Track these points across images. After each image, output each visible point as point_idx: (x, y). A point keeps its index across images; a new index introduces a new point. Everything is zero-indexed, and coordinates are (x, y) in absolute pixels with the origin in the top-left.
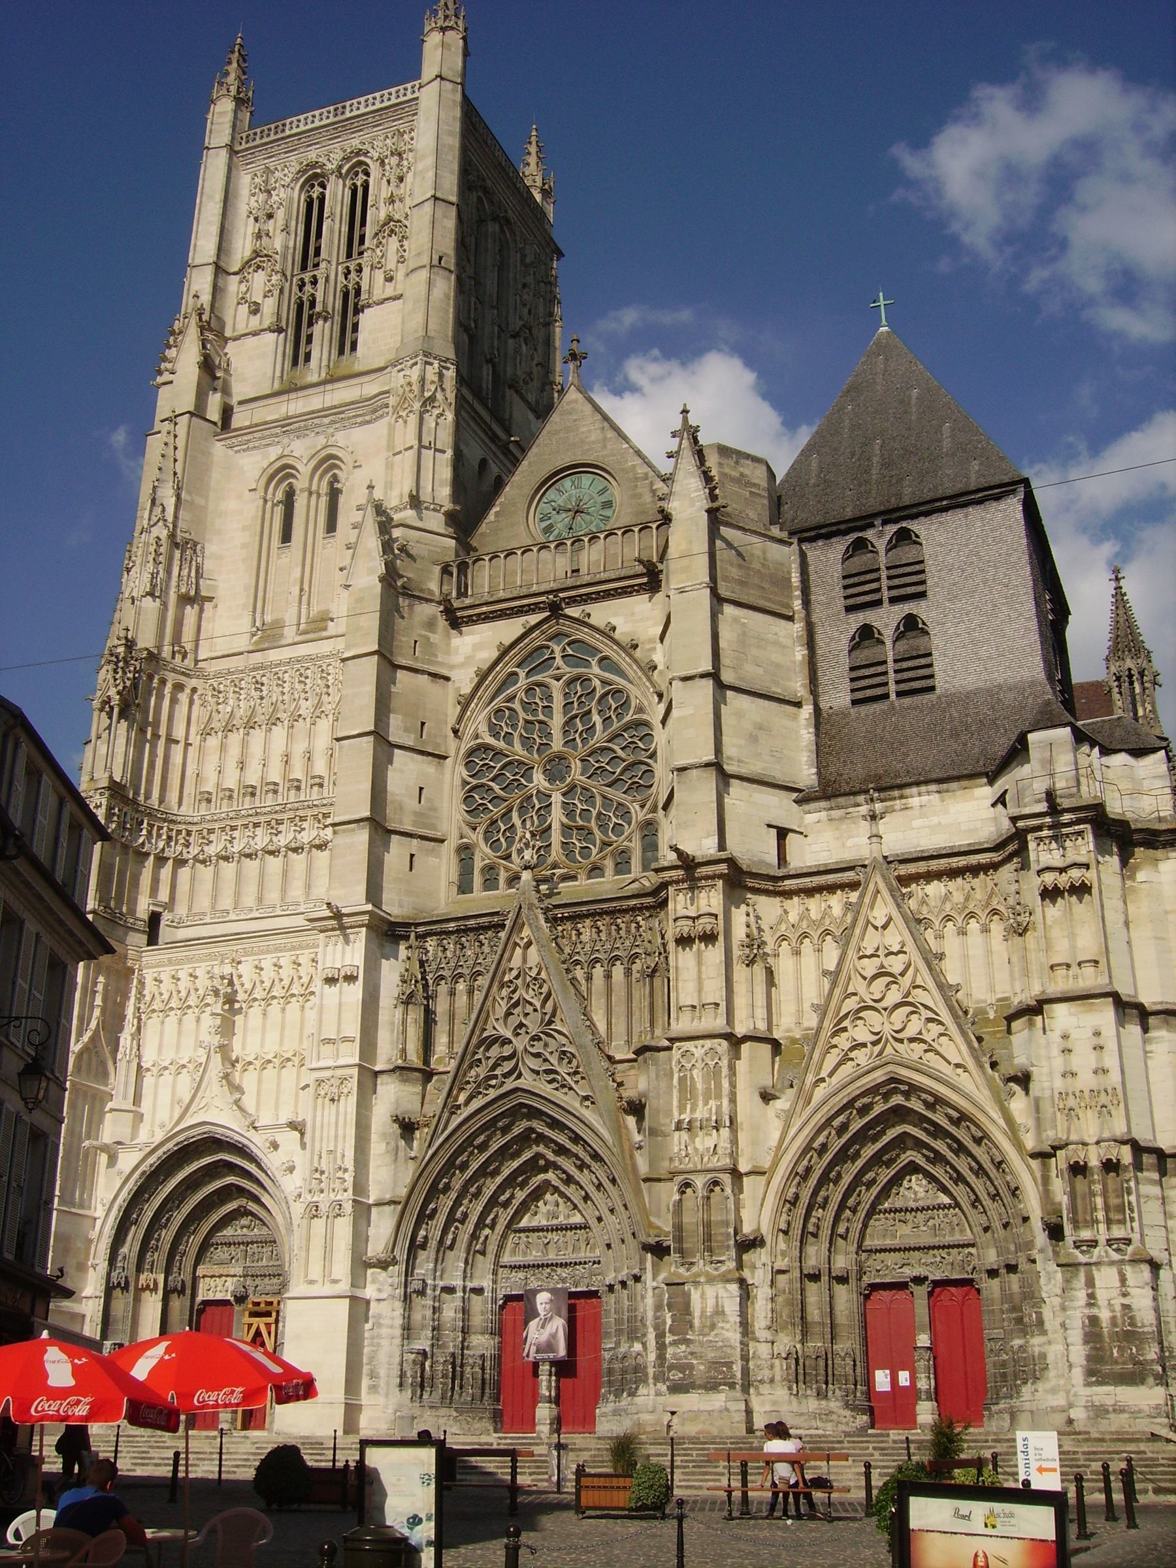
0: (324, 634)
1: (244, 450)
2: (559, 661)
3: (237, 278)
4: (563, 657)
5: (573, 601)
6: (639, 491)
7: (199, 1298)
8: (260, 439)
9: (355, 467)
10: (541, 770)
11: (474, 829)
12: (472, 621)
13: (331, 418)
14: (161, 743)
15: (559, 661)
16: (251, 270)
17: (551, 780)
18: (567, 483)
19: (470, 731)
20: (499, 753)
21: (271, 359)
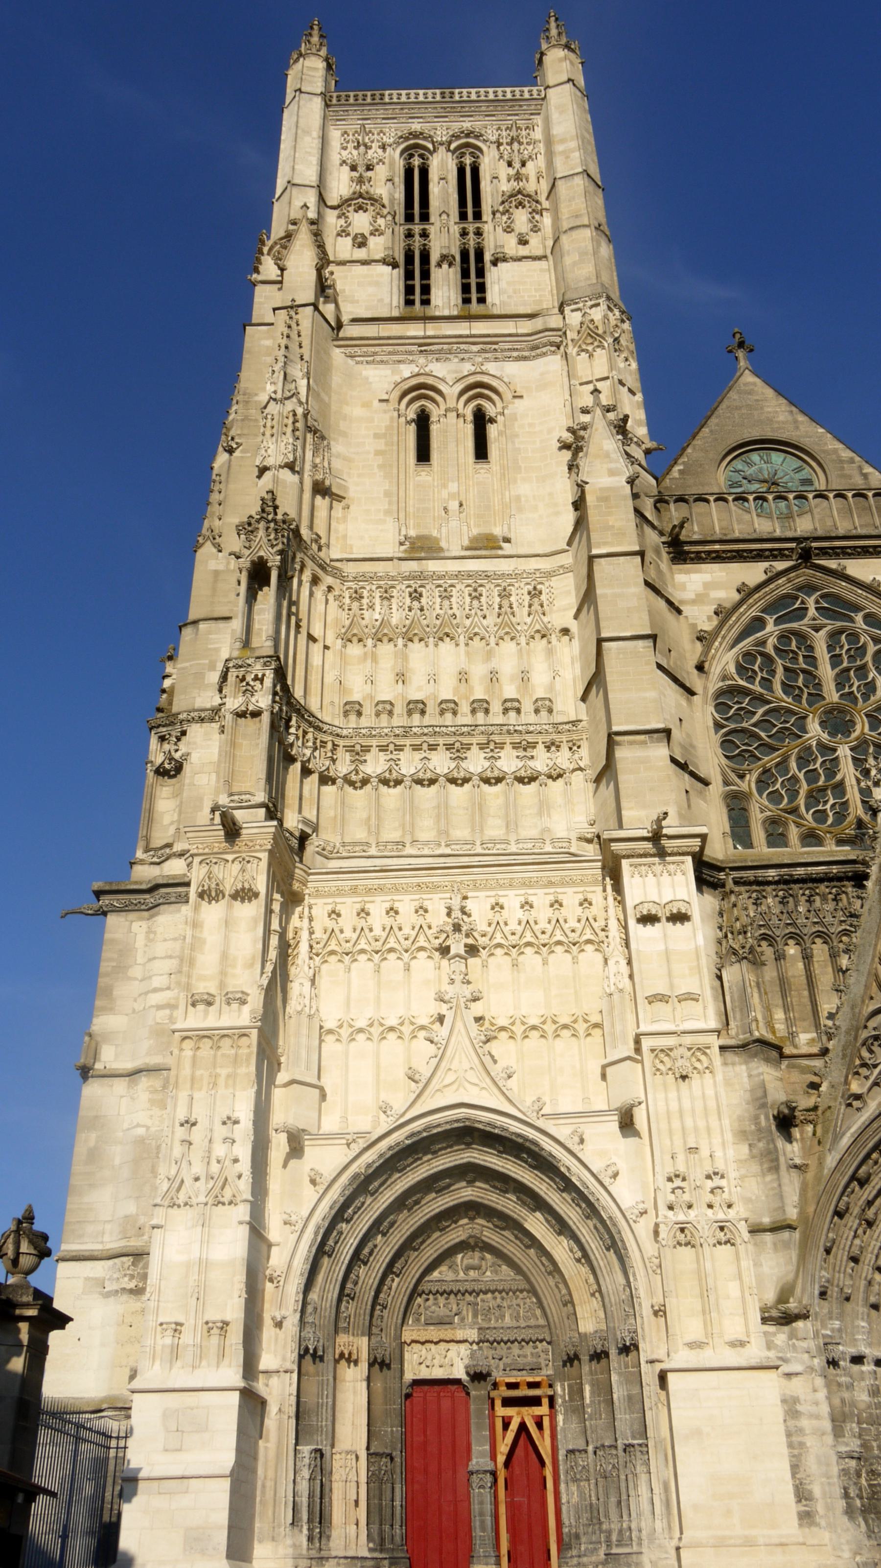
0: (500, 552)
1: (367, 362)
2: (812, 612)
3: (336, 213)
4: (817, 609)
5: (824, 552)
6: (847, 472)
7: (409, 1376)
8: (390, 353)
9: (514, 397)
10: (817, 721)
11: (742, 777)
12: (699, 558)
13: (481, 346)
14: (302, 638)
15: (812, 612)
16: (351, 209)
17: (832, 734)
18: (755, 457)
19: (715, 670)
20: (761, 700)
21: (387, 288)
